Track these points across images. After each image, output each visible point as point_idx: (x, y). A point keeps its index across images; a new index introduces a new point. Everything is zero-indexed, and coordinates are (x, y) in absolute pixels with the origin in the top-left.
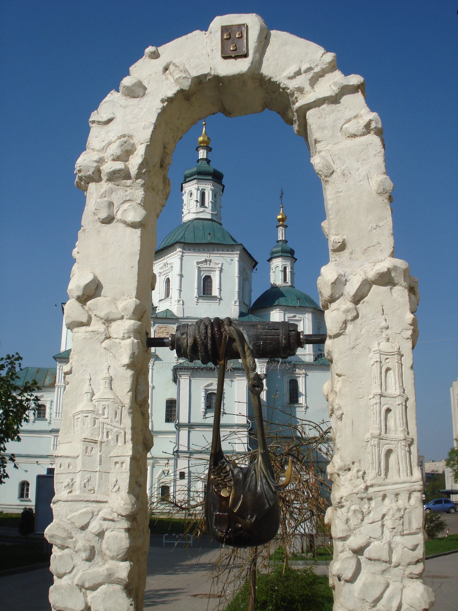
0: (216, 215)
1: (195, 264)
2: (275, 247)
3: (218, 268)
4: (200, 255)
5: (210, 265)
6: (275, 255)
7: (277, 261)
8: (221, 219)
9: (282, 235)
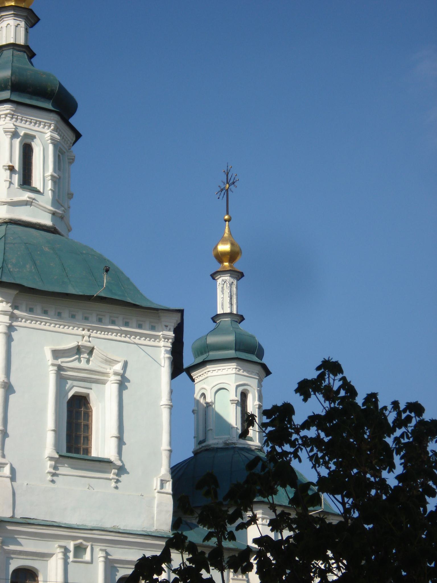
0: (62, 218)
1: (49, 356)
2: (213, 332)
3: (116, 374)
4: (61, 329)
5: (88, 361)
6: (213, 355)
7: (220, 373)
8: (69, 230)
9: (231, 298)
